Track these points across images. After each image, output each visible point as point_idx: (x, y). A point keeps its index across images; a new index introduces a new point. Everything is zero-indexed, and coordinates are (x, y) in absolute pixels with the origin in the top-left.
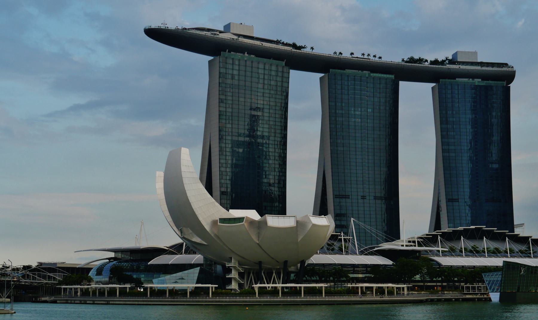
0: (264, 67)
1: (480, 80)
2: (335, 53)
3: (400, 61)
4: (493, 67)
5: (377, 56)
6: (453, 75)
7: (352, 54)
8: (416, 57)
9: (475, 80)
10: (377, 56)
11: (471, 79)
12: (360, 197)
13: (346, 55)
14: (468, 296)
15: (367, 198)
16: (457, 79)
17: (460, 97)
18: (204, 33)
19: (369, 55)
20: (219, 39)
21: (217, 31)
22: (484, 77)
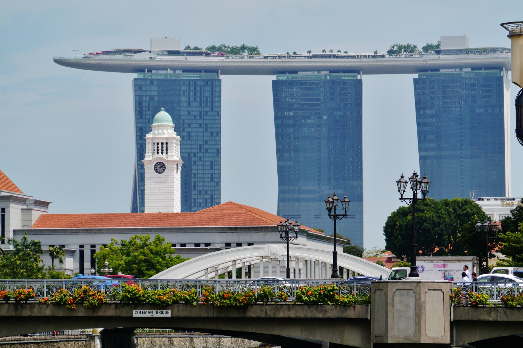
1: (470, 70)
7: (310, 52)
9: (464, 70)
16: (441, 70)
19: (331, 51)
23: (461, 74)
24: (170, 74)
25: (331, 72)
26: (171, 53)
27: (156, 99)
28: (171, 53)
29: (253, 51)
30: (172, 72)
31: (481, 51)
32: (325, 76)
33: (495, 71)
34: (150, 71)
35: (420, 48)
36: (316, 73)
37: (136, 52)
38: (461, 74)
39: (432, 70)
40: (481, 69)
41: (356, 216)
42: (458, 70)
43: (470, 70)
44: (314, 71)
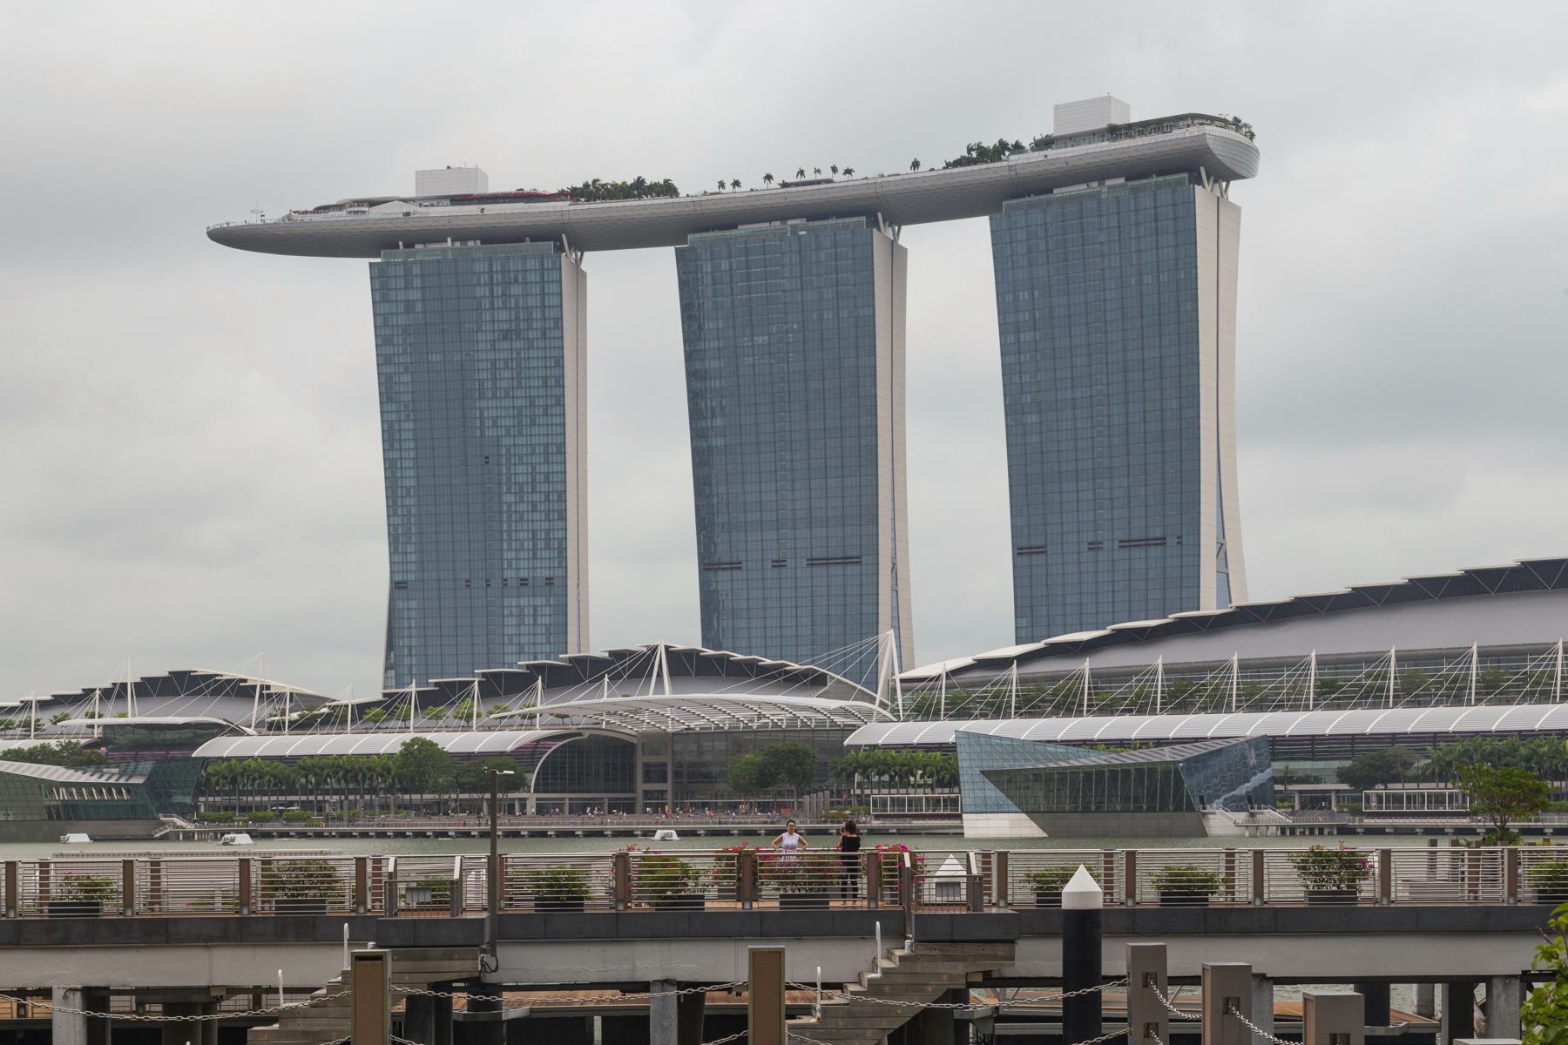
0: (491, 266)
2: (722, 185)
3: (905, 169)
4: (1114, 140)
5: (841, 170)
6: (1037, 186)
7: (769, 177)
8: (990, 143)
10: (841, 170)
11: (1084, 186)
12: (769, 564)
13: (752, 182)
14: (916, 823)
15: (790, 563)
17: (1142, 233)
18: (341, 215)
20: (375, 221)
23: (1099, 193)
24: (453, 249)
26: (457, 200)
27: (419, 307)
28: (457, 200)
29: (668, 189)
30: (458, 244)
32: (795, 229)
33: (1176, 176)
34: (409, 245)
37: (373, 203)
38: (1099, 193)
39: (1037, 194)
40: (1144, 175)
42: (1095, 184)
44: (770, 221)
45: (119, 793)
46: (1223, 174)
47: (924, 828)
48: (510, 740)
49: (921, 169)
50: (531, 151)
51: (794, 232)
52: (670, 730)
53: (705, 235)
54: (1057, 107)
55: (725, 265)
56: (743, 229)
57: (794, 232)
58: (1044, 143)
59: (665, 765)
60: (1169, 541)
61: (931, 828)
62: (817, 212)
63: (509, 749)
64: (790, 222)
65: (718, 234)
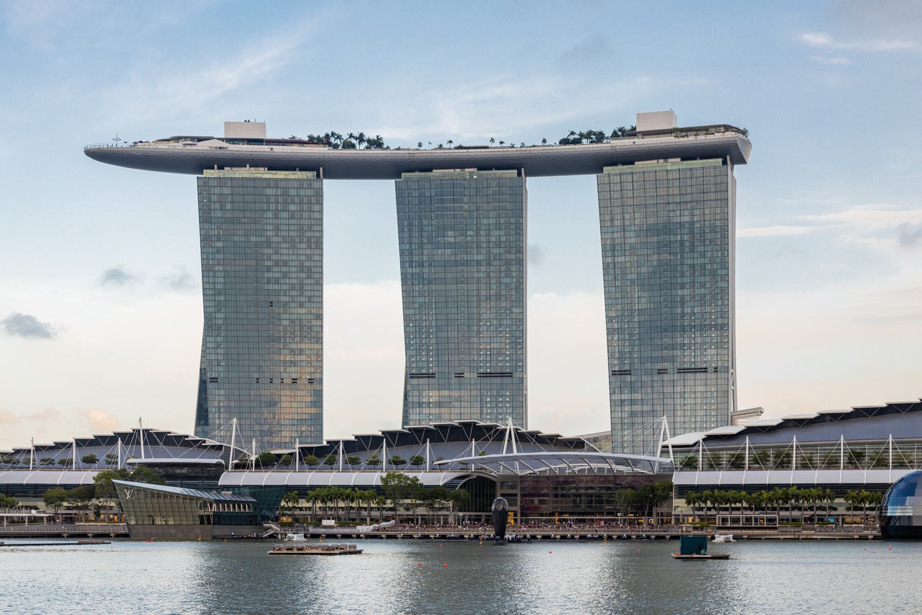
1: (679, 160)
6: (627, 159)
7: (451, 142)
9: (670, 160)
21: (192, 139)
22: (687, 154)
25: (480, 168)
26: (250, 141)
28: (250, 141)
31: (697, 130)
32: (471, 174)
34: (221, 167)
35: (608, 133)
36: (458, 170)
39: (624, 163)
40: (695, 159)
41: (514, 375)
43: (679, 160)
44: (454, 167)
45: (244, 507)
46: (743, 161)
47: (765, 535)
48: (439, 479)
49: (547, 144)
50: (291, 118)
51: (471, 177)
52: (519, 473)
53: (412, 174)
54: (638, 115)
55: (427, 193)
56: (436, 172)
57: (471, 177)
58: (633, 133)
59: (516, 495)
60: (709, 370)
61: (770, 535)
62: (484, 165)
63: (441, 483)
64: (466, 170)
65: (422, 174)
